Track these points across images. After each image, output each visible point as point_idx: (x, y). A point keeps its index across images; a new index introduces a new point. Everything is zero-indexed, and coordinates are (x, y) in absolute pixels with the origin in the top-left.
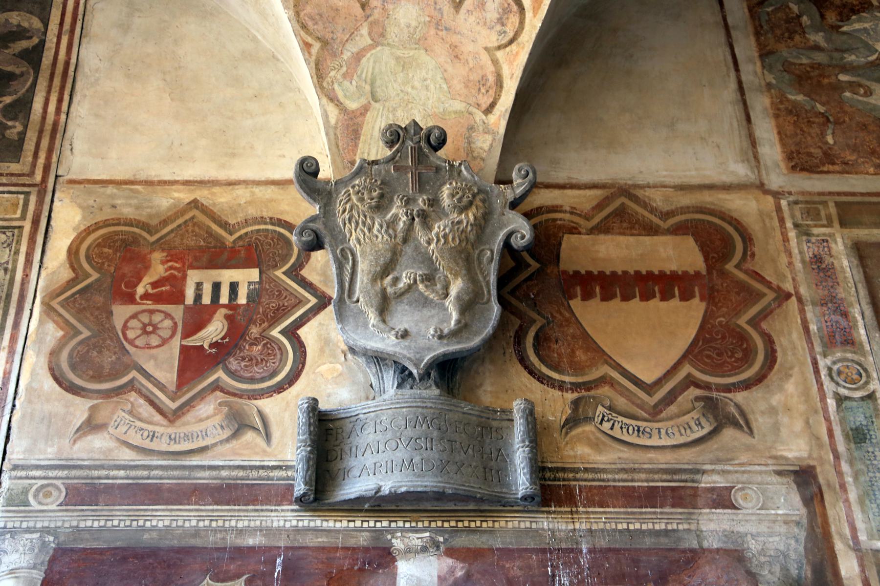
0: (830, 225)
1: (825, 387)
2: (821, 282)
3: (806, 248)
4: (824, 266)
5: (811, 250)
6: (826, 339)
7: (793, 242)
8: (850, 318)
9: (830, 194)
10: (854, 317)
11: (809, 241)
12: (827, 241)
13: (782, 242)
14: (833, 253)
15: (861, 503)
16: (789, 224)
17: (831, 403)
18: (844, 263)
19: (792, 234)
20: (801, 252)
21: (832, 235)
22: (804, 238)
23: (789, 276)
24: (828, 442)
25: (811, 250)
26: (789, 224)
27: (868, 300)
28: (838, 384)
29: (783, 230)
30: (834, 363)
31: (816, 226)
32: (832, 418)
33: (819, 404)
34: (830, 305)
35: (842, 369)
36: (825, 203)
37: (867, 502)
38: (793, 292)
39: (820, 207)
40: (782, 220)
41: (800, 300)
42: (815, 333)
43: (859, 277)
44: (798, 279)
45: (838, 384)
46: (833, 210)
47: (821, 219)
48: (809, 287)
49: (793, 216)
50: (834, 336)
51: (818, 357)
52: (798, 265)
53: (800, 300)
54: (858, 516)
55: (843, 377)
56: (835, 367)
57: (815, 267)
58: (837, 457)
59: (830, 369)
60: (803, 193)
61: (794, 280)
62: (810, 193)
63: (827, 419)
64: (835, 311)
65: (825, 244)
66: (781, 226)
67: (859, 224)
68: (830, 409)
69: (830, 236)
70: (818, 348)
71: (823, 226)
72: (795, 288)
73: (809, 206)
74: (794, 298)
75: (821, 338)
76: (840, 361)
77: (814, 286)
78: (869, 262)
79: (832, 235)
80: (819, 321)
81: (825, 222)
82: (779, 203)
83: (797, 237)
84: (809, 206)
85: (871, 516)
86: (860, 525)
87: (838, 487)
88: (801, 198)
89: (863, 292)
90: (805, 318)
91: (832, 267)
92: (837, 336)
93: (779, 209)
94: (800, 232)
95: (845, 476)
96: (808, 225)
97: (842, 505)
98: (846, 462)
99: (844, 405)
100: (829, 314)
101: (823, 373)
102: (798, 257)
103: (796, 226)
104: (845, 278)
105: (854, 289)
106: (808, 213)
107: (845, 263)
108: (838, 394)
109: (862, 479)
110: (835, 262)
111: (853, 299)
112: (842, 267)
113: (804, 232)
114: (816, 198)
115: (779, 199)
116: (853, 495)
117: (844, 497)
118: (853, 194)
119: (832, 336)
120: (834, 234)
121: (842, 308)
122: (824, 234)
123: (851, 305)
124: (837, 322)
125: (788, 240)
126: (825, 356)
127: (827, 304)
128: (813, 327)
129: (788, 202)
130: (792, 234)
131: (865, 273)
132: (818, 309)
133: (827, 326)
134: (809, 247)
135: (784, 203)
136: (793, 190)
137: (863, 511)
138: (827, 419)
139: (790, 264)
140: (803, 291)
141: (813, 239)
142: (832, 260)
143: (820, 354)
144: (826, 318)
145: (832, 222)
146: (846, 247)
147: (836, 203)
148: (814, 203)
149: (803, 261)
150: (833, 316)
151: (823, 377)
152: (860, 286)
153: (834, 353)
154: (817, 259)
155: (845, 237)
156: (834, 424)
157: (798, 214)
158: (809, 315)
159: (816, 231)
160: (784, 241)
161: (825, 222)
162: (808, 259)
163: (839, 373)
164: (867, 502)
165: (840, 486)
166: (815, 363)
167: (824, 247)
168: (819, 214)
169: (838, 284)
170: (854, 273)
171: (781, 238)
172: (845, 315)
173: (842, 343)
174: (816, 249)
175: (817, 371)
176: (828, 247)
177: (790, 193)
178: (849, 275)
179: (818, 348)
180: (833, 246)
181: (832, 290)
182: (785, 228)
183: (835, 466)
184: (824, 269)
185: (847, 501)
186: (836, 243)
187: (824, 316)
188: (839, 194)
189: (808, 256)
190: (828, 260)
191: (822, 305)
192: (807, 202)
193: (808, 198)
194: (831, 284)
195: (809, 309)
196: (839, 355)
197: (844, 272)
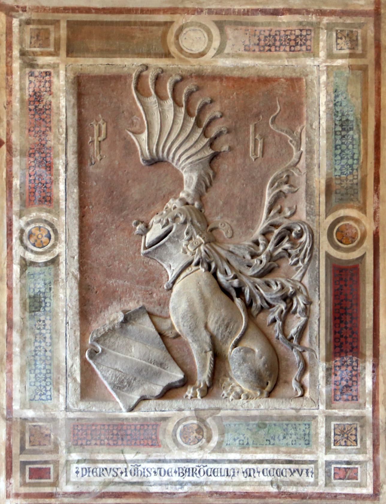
0: (55, 54)
1: (14, 251)
2: (34, 127)
3: (27, 83)
4: (41, 106)
5: (32, 85)
6: (26, 197)
7: (16, 76)
8: (54, 171)
9: (66, 10)
10: (58, 170)
11: (32, 74)
12: (50, 74)
13: (5, 76)
14: (54, 90)
15: (22, 373)
16: (16, 53)
17: (16, 268)
18: (62, 102)
19: (16, 65)
20: (22, 89)
21: (55, 66)
22: (28, 70)
23: (5, 120)
24: (5, 312)
25: (32, 85)
26: (16, 53)
27: (75, 149)
28: (26, 248)
29: (9, 59)
30: (28, 224)
31: (43, 54)
32: (14, 285)
33: (5, 271)
34: (37, 155)
35: (33, 231)
36: (56, 23)
37: (27, 372)
38: (4, 140)
39: (51, 28)
40: (9, 46)
41: (10, 150)
42: (17, 189)
43: (73, 120)
44: (13, 122)
45: (26, 248)
46: (63, 32)
47: (48, 46)
48: (21, 133)
49: (21, 41)
50: (34, 193)
51: (14, 218)
52: (16, 105)
53: (10, 150)
54: (17, 385)
55: (32, 240)
56: (27, 230)
57: (32, 107)
58: (10, 327)
59: (22, 231)
60: (37, 9)
61: (8, 124)
62: (44, 9)
63: (10, 288)
64: (41, 162)
65: (47, 78)
66: (7, 54)
67: (86, 52)
68: (14, 276)
69: (54, 68)
70: (16, 208)
71: (50, 54)
72: (7, 134)
73: (40, 27)
74: (4, 147)
75: (21, 195)
76: (33, 221)
77: (27, 131)
78: (86, 101)
79: (55, 66)
80: (23, 175)
81: (51, 49)
82: (11, 23)
83: (21, 69)
84: (40, 27)
85: (28, 385)
86: (17, 396)
87: (5, 357)
88: (34, 16)
89: (73, 138)
90: (11, 171)
91: (48, 108)
92: (37, 193)
93: (9, 31)
94: (25, 62)
95: (14, 346)
96: (34, 54)
97: (5, 375)
98: (17, 331)
99: (27, 272)
100: (35, 166)
101: (16, 235)
102: (18, 96)
103: (23, 53)
104: (59, 121)
105: (64, 135)
106: (38, 36)
107: (63, 102)
108: (24, 259)
109: (28, 349)
110: (53, 101)
111: (61, 148)
112: (58, 108)
113: (28, 61)
114: (50, 17)
115: (12, 17)
116: (16, 366)
117: (9, 367)
118: (88, 10)
119: (32, 193)
120: (58, 64)
121: (48, 159)
122: (49, 65)
123: (57, 155)
124: (40, 176)
125: (11, 74)
126: (20, 217)
127: (34, 154)
128: (16, 182)
129: (21, 21)
130: (16, 65)
131: (80, 114)
132: (25, 159)
133: (30, 181)
134: (31, 82)
135: (16, 22)
136: (28, 4)
137: (22, 381)
138: (10, 288)
139: (9, 103)
140: (15, 138)
141: (37, 72)
142: (50, 98)
143: (17, 215)
144: (31, 171)
145: (59, 49)
146: (67, 82)
147: (68, 22)
148: (46, 22)
149: (22, 101)
150: (37, 169)
151: (14, 240)
152: (71, 131)
153: (30, 213)
154: (37, 97)
155: (69, 68)
156: (14, 291)
157: (27, 38)
158: (16, 168)
159: (42, 60)
160: (7, 74)
161: (51, 49)
162: (27, 97)
163: (30, 235)
164: (27, 372)
165: (7, 357)
166: (10, 225)
167: (46, 82)
168: (48, 38)
169: (50, 128)
170: (69, 114)
171: (5, 69)
172: (49, 167)
173: (40, 201)
174: (37, 84)
175: (10, 234)
176: (50, 82)
177: (24, 9)
178: (63, 117)
179: (16, 208)
180: (54, 80)
181: (43, 137)
182: (11, 57)
183: (7, 336)
184: (41, 109)
185: (10, 371)
186: (58, 76)
187: (29, 168)
188: (74, 10)
189: (29, 92)
190: (47, 98)
191: (30, 155)
192: (39, 22)
193: (41, 16)
194: (43, 129)
195: (16, 160)
196: (34, 215)
197: (59, 114)
